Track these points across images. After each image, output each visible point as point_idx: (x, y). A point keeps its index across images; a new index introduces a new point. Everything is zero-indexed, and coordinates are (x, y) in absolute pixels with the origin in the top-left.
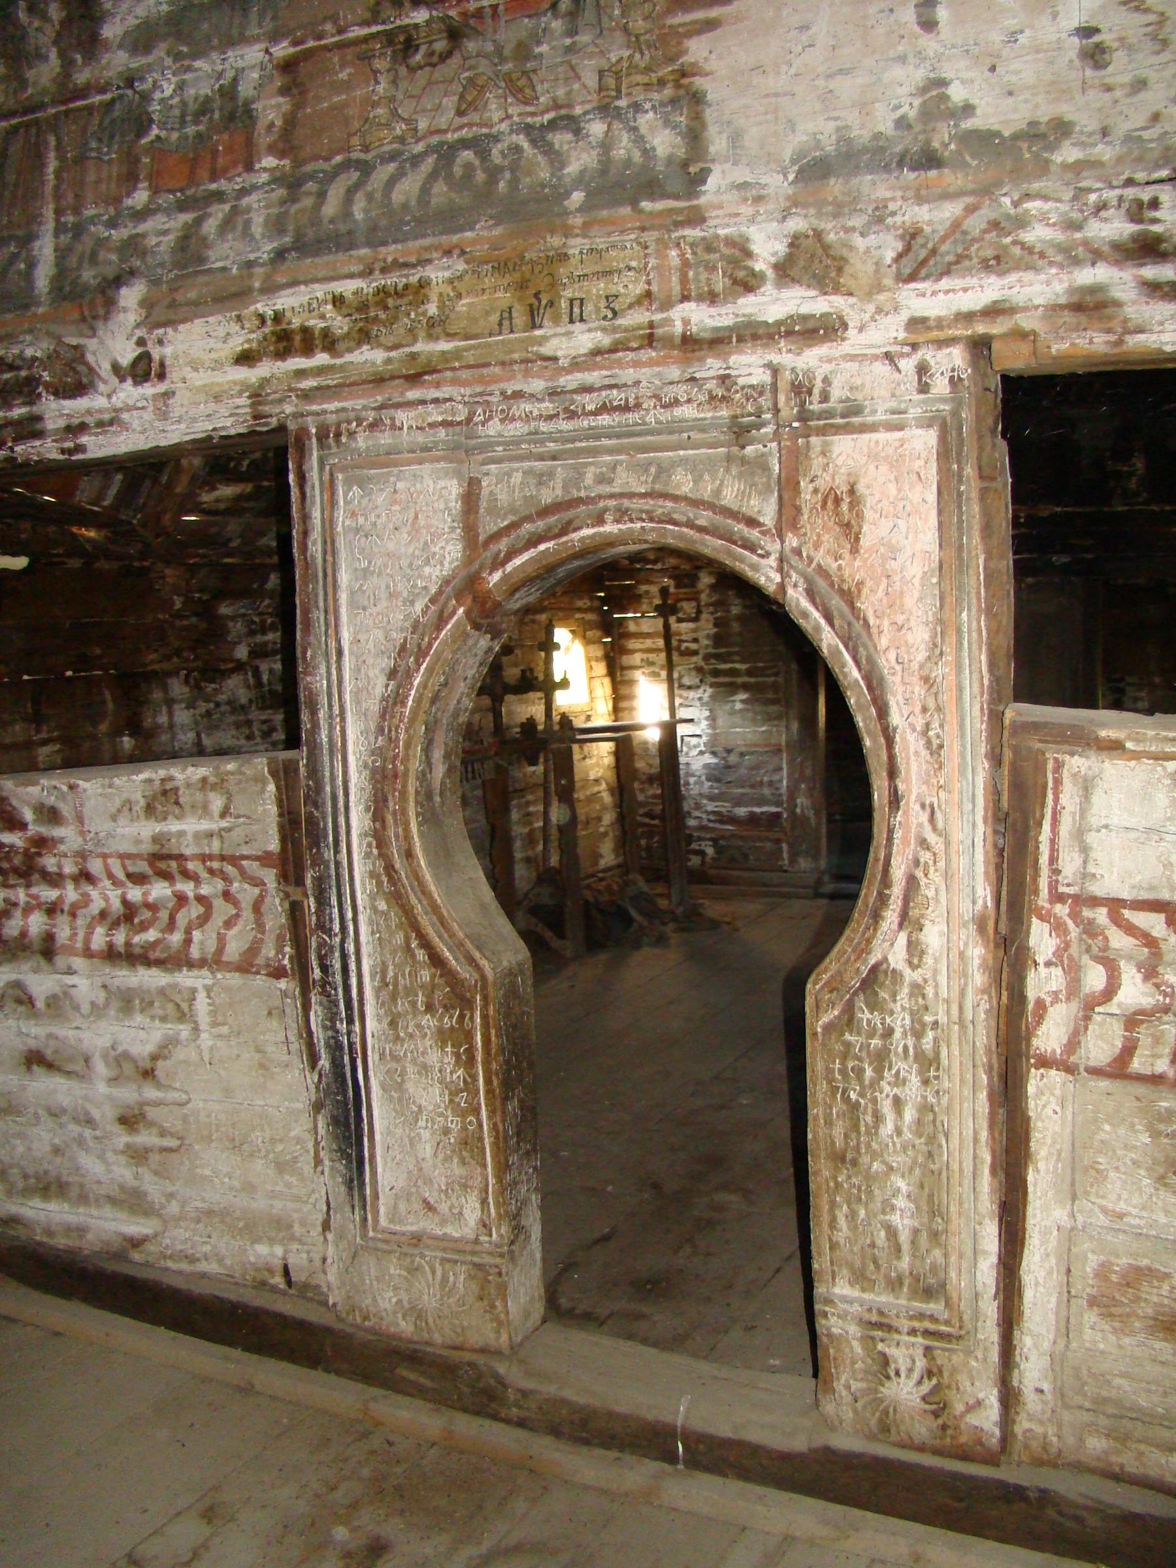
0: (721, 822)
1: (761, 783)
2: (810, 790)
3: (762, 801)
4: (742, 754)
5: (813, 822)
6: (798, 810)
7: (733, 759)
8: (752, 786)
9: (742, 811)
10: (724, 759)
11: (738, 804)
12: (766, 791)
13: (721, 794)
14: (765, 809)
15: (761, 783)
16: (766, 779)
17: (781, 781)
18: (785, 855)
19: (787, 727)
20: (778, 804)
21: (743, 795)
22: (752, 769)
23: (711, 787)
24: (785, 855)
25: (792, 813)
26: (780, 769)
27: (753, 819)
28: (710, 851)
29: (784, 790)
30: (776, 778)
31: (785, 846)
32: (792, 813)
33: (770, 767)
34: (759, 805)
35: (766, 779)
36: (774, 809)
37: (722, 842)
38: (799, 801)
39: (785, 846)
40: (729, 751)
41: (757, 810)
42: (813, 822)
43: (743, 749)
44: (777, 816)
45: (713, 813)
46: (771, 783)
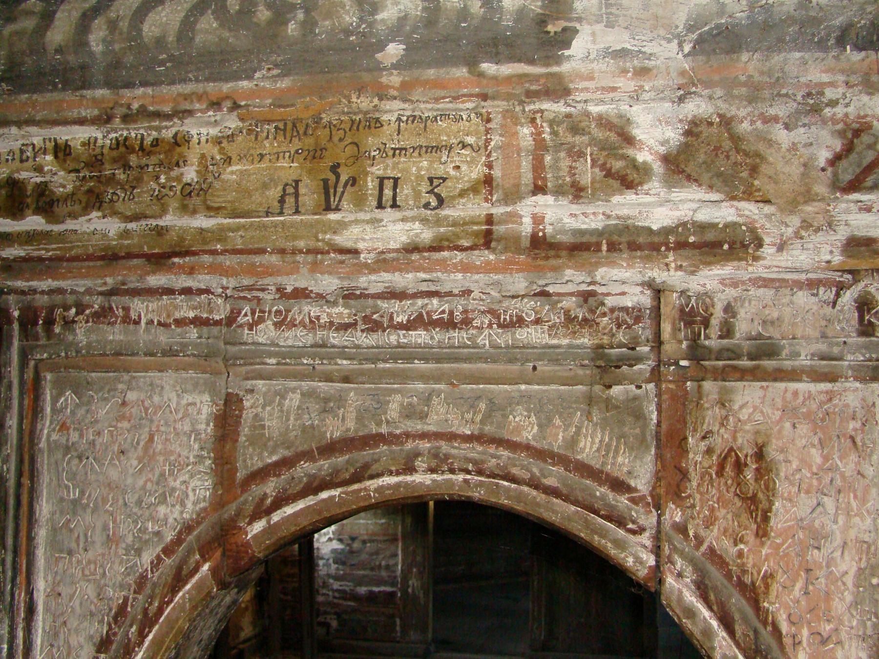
0: (345, 599)
1: (380, 566)
2: (420, 573)
3: (380, 582)
4: (364, 542)
5: (422, 602)
6: (410, 590)
7: (356, 545)
8: (372, 569)
9: (363, 590)
10: (348, 545)
11: (360, 584)
12: (384, 573)
13: (345, 574)
14: (382, 588)
15: (380, 566)
16: (383, 563)
17: (396, 564)
18: (398, 628)
19: (403, 521)
20: (393, 584)
21: (364, 576)
22: (372, 554)
23: (337, 569)
24: (398, 628)
25: (405, 591)
26: (396, 555)
27: (372, 597)
28: (334, 624)
29: (399, 573)
30: (391, 562)
31: (398, 621)
32: (405, 591)
33: (388, 553)
34: (378, 585)
35: (383, 563)
36: (389, 589)
37: (344, 616)
38: (410, 582)
39: (398, 621)
40: (353, 539)
41: (376, 589)
42: (422, 602)
43: (366, 537)
44: (392, 594)
45: (337, 591)
46: (388, 567)
